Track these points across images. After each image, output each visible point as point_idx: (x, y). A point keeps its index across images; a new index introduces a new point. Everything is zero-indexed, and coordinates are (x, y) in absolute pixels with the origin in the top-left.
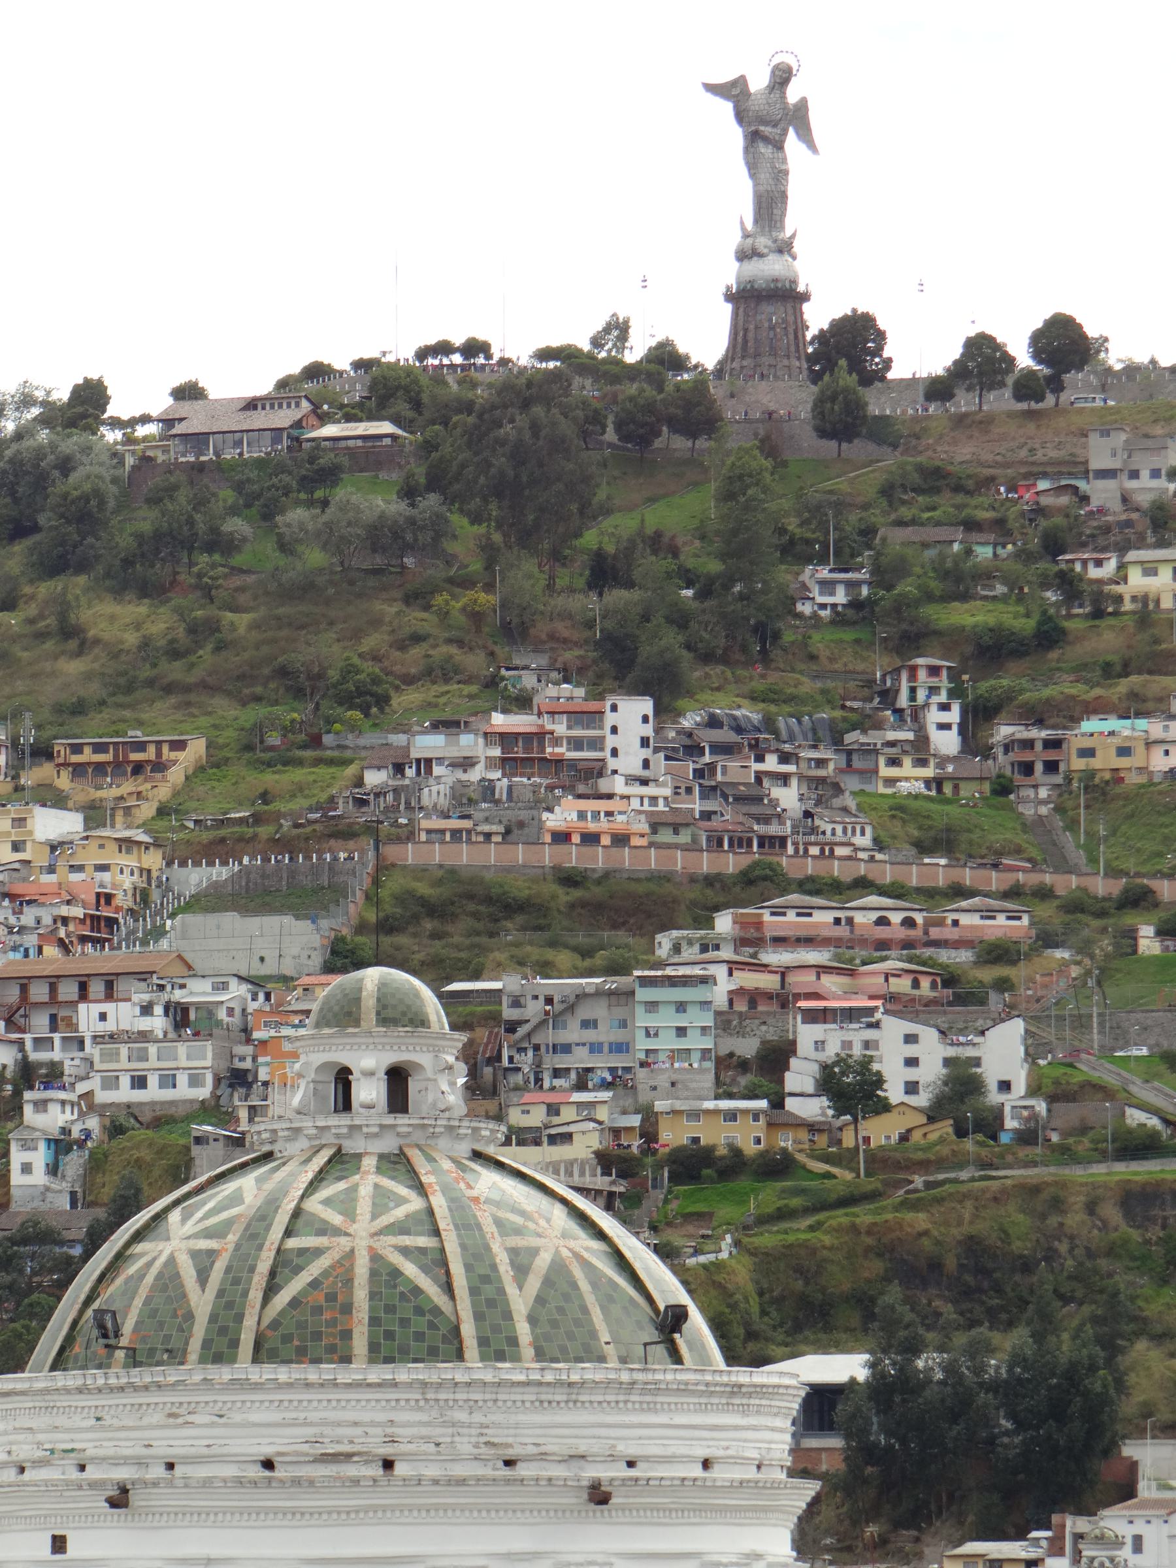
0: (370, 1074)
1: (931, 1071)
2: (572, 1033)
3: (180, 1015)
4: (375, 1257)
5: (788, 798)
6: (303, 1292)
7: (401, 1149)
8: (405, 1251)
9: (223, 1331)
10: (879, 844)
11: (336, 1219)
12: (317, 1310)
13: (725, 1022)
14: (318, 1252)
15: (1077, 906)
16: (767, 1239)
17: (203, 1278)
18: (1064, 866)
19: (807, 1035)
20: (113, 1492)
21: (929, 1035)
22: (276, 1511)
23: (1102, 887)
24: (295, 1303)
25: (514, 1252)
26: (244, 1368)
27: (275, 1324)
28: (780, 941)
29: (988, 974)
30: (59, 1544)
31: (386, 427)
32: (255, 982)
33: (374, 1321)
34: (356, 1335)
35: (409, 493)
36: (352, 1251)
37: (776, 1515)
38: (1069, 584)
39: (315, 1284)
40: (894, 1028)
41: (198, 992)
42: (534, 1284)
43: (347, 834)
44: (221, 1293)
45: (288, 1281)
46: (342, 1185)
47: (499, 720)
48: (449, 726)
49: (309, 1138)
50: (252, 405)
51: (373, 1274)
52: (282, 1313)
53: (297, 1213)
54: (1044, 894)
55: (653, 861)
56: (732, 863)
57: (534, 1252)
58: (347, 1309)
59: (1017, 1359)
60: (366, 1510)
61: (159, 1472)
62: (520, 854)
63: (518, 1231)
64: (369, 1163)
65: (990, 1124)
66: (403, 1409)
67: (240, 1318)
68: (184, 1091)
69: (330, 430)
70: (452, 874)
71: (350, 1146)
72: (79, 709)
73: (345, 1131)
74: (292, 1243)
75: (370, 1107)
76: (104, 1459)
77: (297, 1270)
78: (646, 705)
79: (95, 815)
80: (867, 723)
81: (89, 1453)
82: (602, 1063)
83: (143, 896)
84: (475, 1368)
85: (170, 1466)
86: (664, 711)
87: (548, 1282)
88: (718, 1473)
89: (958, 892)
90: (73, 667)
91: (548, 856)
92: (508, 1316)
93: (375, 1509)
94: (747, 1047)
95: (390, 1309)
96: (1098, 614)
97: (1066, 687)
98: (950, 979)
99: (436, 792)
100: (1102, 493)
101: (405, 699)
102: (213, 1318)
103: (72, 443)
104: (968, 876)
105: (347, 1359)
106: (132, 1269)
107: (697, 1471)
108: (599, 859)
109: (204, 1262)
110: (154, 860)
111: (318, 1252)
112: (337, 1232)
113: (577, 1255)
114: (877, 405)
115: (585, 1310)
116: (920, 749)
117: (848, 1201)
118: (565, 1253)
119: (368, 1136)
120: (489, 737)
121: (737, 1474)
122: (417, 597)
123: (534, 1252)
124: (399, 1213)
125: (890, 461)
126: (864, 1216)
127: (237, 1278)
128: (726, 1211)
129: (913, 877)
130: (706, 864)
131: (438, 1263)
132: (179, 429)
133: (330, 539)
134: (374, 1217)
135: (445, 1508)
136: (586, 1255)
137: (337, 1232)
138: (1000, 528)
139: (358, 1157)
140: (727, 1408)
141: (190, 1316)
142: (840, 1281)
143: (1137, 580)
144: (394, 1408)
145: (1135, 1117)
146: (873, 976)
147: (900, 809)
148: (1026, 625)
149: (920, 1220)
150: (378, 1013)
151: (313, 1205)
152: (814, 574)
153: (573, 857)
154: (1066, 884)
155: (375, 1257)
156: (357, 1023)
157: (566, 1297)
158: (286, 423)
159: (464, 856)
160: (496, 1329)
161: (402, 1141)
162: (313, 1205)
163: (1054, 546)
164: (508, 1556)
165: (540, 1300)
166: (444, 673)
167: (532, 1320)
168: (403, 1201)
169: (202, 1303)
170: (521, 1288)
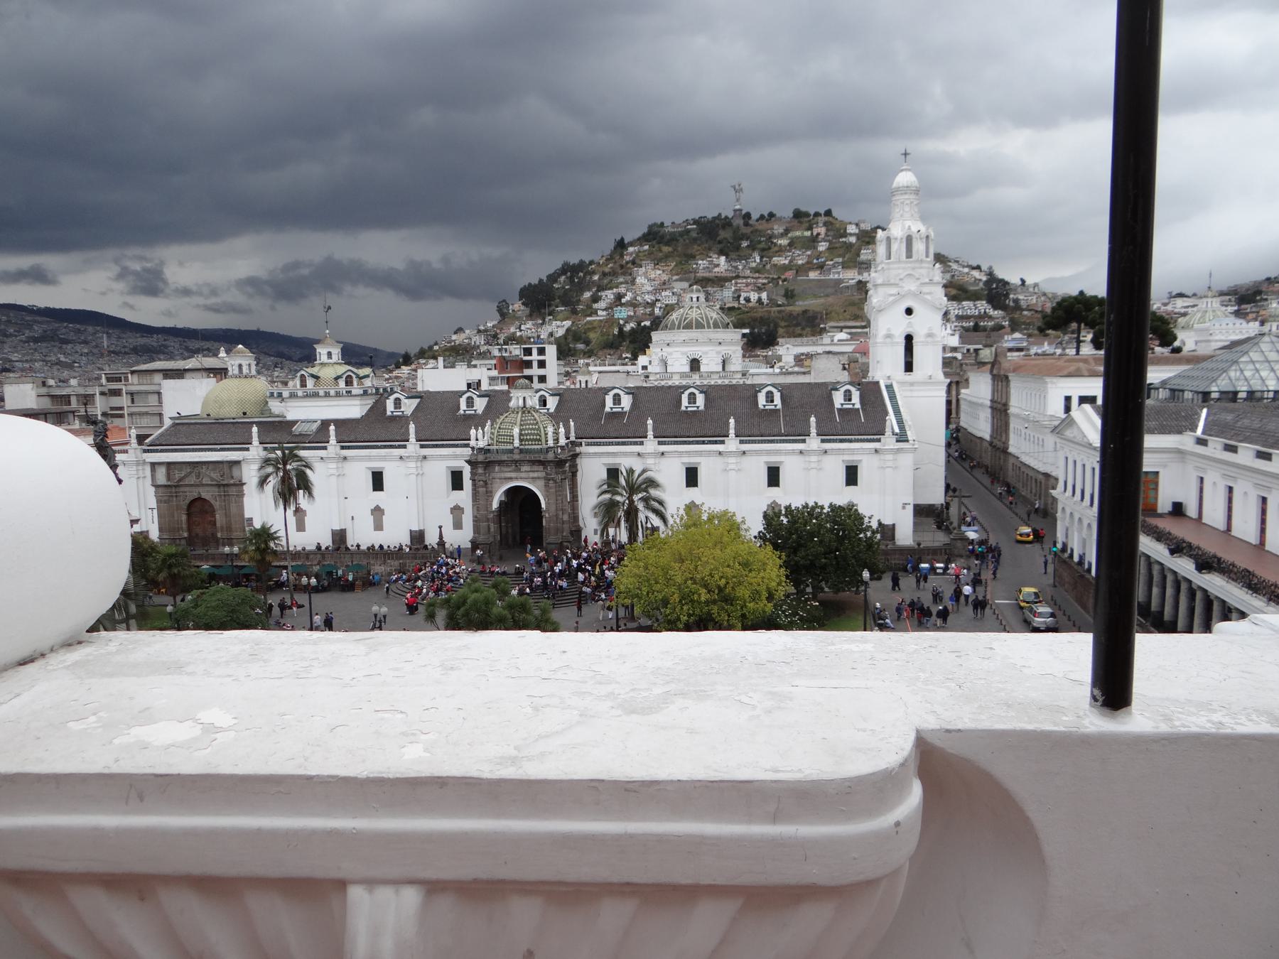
1: (756, 298)
2: (716, 294)
3: (673, 293)
5: (740, 267)
10: (751, 272)
13: (734, 293)
15: (773, 279)
16: (739, 317)
18: (771, 274)
19: (742, 294)
21: (756, 294)
23: (775, 277)
28: (740, 283)
29: (763, 286)
31: (695, 226)
32: (681, 289)
35: (698, 234)
38: (772, 243)
40: (752, 293)
41: (675, 290)
43: (691, 272)
47: (708, 259)
48: (703, 260)
54: (769, 278)
55: (726, 275)
56: (734, 275)
59: (766, 330)
62: (710, 274)
65: (763, 303)
68: (674, 302)
69: (689, 227)
70: (703, 277)
72: (662, 259)
78: (724, 257)
79: (663, 271)
80: (749, 259)
82: (720, 298)
83: (669, 280)
86: (727, 258)
89: (759, 278)
90: (661, 254)
91: (713, 275)
94: (736, 296)
96: (775, 246)
97: (771, 254)
98: (758, 287)
99: (701, 268)
100: (776, 232)
101: (697, 257)
103: (659, 229)
104: (760, 276)
108: (719, 275)
109: (677, 319)
110: (670, 276)
114: (751, 222)
116: (755, 261)
117: (747, 312)
120: (707, 261)
122: (699, 245)
125: (752, 229)
126: (749, 314)
127: (681, 320)
128: (733, 314)
129: (754, 276)
130: (731, 275)
131: (702, 318)
133: (688, 239)
138: (764, 236)
142: (747, 321)
143: (779, 242)
145: (779, 303)
146: (750, 287)
147: (753, 268)
148: (767, 247)
149: (755, 314)
152: (743, 242)
153: (716, 275)
154: (771, 276)
159: (705, 275)
163: (770, 238)
166: (702, 254)
169: (677, 323)
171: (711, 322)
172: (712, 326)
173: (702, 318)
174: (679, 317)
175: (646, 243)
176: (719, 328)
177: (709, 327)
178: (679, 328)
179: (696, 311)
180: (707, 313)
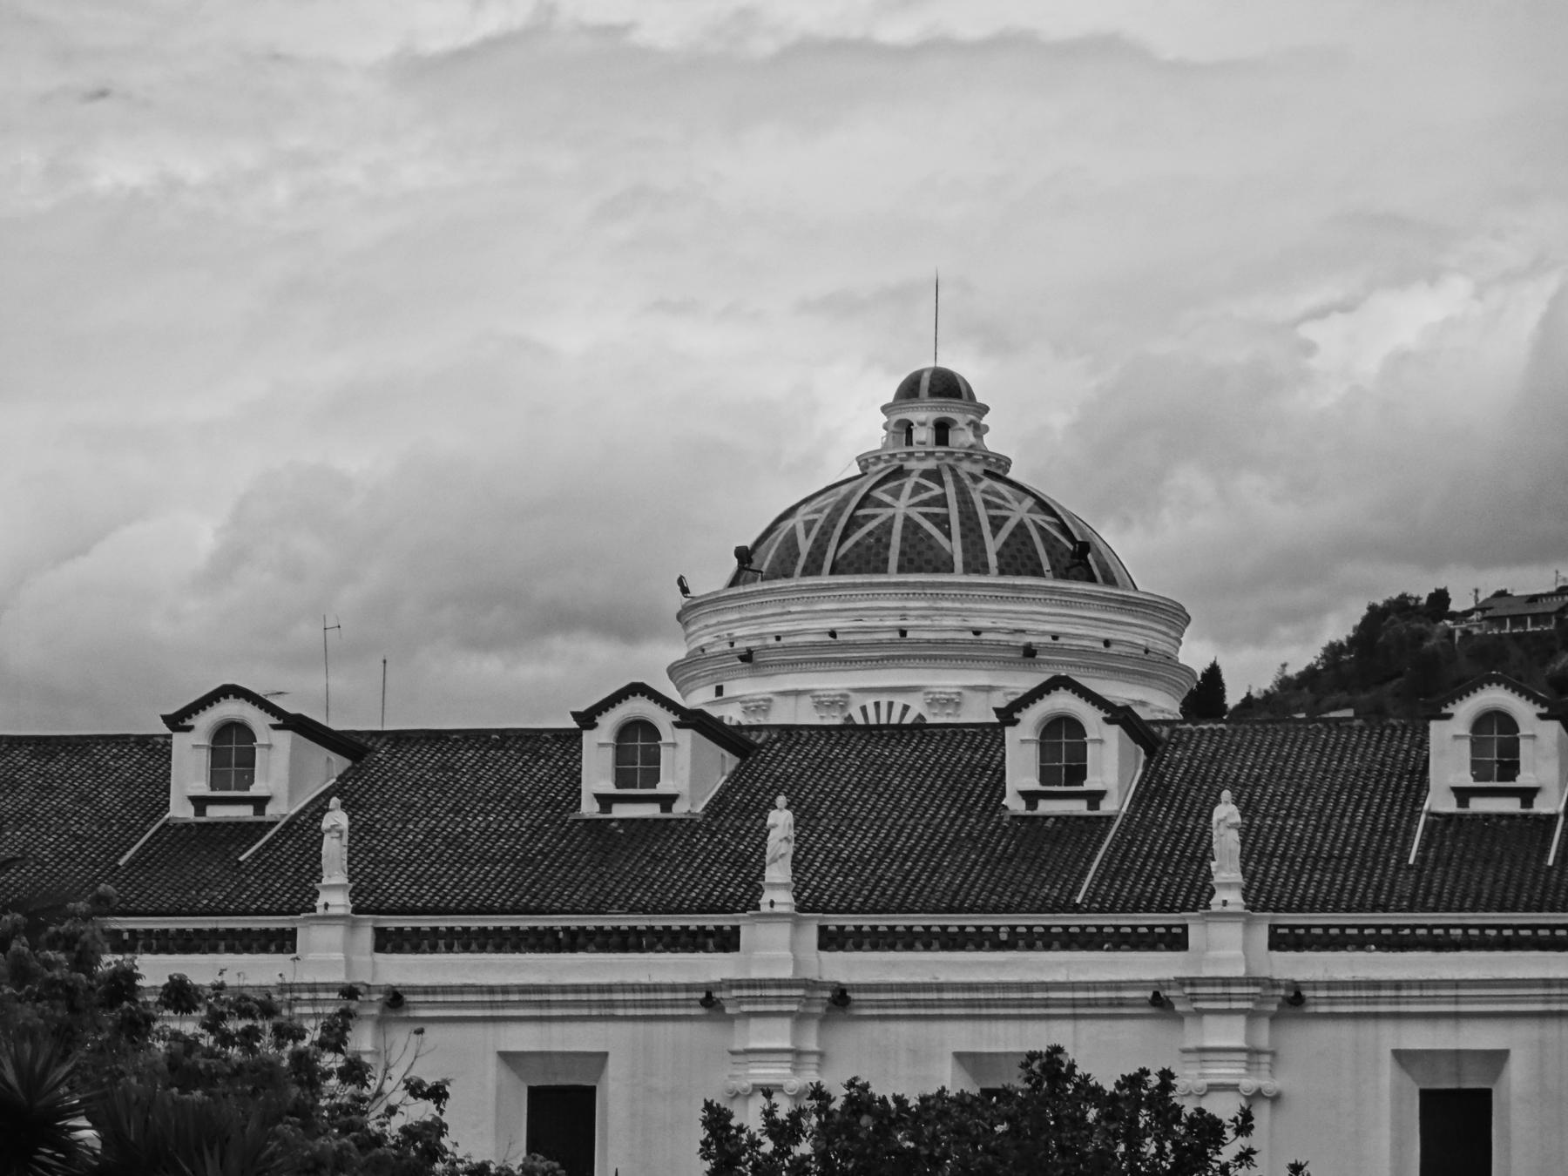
0: (922, 424)
4: (907, 519)
6: (864, 538)
7: (938, 466)
8: (925, 515)
9: (814, 561)
11: (887, 499)
12: (869, 548)
14: (874, 517)
17: (808, 533)
20: (744, 652)
22: (840, 660)
24: (857, 544)
25: (992, 519)
26: (825, 579)
27: (845, 556)
30: (719, 691)
33: (902, 553)
34: (890, 561)
36: (894, 516)
37: (1156, 681)
39: (870, 534)
42: (1004, 534)
44: (816, 540)
45: (854, 532)
46: (896, 483)
49: (886, 461)
50: (1533, 599)
51: (905, 527)
52: (850, 550)
57: (1006, 518)
58: (887, 546)
60: (888, 658)
61: (772, 641)
63: (999, 507)
64: (916, 474)
66: (911, 599)
67: (824, 553)
71: (908, 465)
73: (904, 456)
74: (861, 512)
75: (923, 443)
76: (742, 637)
77: (862, 526)
81: (736, 635)
84: (958, 577)
85: (778, 638)
87: (1013, 534)
88: (1113, 649)
92: (984, 551)
95: (913, 546)
102: (810, 554)
105: (884, 571)
106: (772, 536)
109: (809, 526)
111: (874, 517)
112: (888, 505)
115: (1035, 552)
118: (1027, 521)
119: (920, 459)
123: (1006, 518)
124: (925, 496)
127: (825, 533)
131: (942, 522)
132: (1488, 613)
134: (911, 497)
135: (935, 658)
136: (1047, 527)
137: (888, 505)
139: (912, 471)
140: (1120, 611)
141: (798, 554)
144: (906, 599)
150: (930, 390)
151: (878, 494)
155: (907, 519)
161: (939, 462)
162: (878, 494)
164: (974, 688)
165: (1006, 544)
167: (999, 554)
168: (931, 489)
169: (805, 546)
170: (994, 536)
171: (992, 546)
172: (992, 560)
173: (942, 522)
174: (821, 518)
175: (1344, 696)
176: (1037, 572)
177: (976, 564)
178: (813, 568)
179: (918, 489)
180: (977, 498)
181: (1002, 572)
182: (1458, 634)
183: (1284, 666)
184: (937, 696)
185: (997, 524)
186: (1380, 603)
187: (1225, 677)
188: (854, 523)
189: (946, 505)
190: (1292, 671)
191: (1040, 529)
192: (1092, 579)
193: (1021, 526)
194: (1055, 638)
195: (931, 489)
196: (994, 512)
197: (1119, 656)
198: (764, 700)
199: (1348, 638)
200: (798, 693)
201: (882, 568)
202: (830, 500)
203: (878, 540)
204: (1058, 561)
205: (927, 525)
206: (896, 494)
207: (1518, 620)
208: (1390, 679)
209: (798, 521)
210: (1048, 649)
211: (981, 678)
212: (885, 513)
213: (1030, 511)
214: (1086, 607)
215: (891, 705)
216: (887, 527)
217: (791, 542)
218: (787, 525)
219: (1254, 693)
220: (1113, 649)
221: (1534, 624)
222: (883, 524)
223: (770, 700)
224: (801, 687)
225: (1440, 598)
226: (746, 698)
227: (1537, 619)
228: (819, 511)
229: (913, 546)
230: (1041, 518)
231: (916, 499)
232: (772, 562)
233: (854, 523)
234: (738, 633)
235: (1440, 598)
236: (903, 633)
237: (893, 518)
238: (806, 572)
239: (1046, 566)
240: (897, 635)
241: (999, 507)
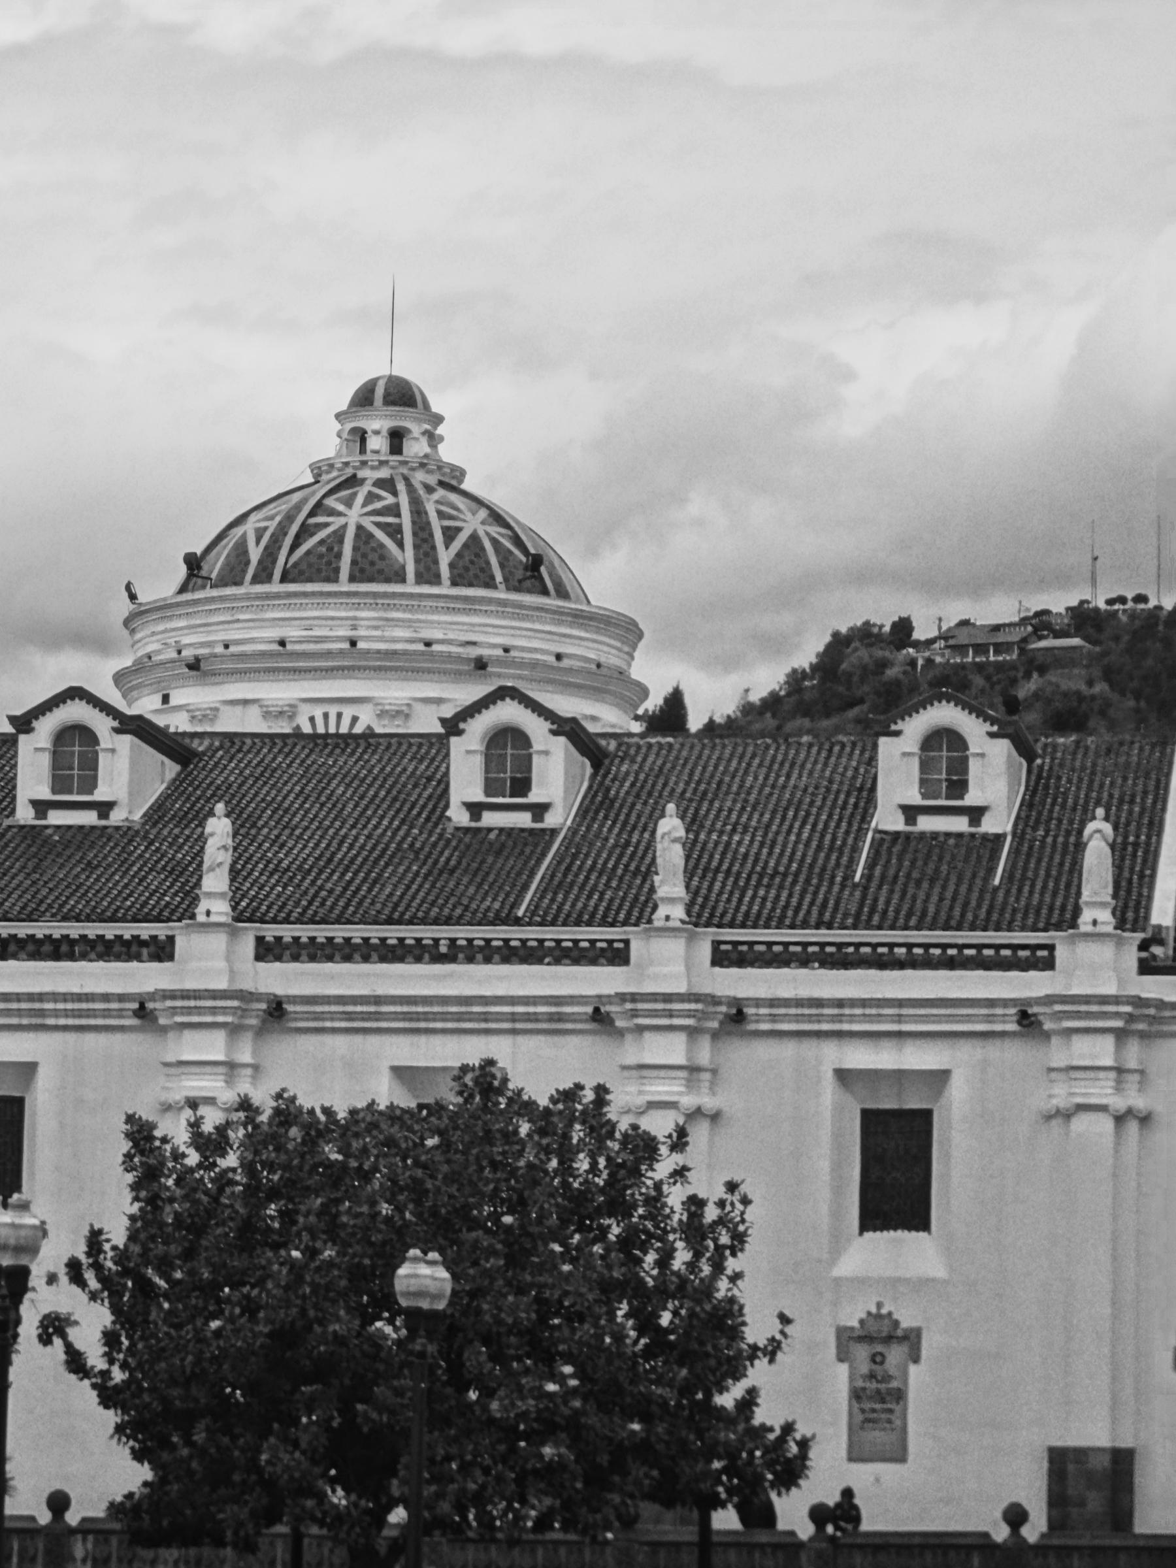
0: (377, 433)
4: (360, 528)
8: (378, 525)
9: (264, 569)
11: (341, 508)
12: (321, 556)
14: (327, 525)
17: (258, 542)
20: (192, 660)
24: (308, 553)
26: (275, 587)
27: (295, 565)
30: (166, 699)
31: (1076, 641)
33: (354, 562)
39: (322, 542)
42: (457, 545)
44: (266, 548)
49: (340, 470)
50: (997, 628)
51: (357, 536)
52: (301, 559)
53: (319, 505)
57: (459, 530)
58: (339, 556)
61: (219, 649)
63: (451, 518)
64: (369, 482)
69: (1043, 644)
71: (361, 474)
74: (312, 521)
75: (377, 452)
76: (190, 645)
77: (312, 535)
84: (411, 588)
85: (226, 646)
87: (466, 546)
88: (566, 663)
93: (343, 668)
95: (364, 556)
102: (260, 562)
107: (552, 659)
111: (327, 525)
112: (340, 514)
113: (488, 534)
115: (488, 563)
118: (481, 533)
119: (373, 468)
121: (577, 664)
124: (378, 505)
131: (395, 532)
132: (951, 642)
137: (340, 514)
140: (571, 625)
141: (248, 562)
150: (384, 397)
151: (331, 502)
155: (360, 528)
156: (371, 404)
157: (477, 555)
158: (1016, 639)
160: (428, 569)
162: (331, 502)
165: (459, 555)
167: (452, 566)
168: (385, 499)
170: (447, 548)
171: (445, 557)
173: (395, 532)
174: (273, 525)
176: (490, 584)
177: (427, 574)
178: (263, 575)
179: (371, 497)
180: (431, 509)
181: (454, 583)
182: (920, 662)
183: (747, 691)
184: (387, 707)
185: (450, 534)
186: (844, 630)
187: (688, 701)
188: (305, 531)
189: (398, 515)
190: (755, 697)
191: (495, 542)
192: (545, 592)
193: (474, 538)
194: (506, 650)
195: (385, 499)
196: (447, 523)
197: (570, 670)
198: (211, 709)
199: (811, 664)
200: (246, 702)
201: (333, 577)
202: (284, 506)
203: (330, 549)
204: (511, 573)
205: (380, 535)
206: (349, 503)
207: (980, 649)
208: (851, 705)
209: (249, 527)
210: (499, 662)
211: (430, 690)
212: (337, 522)
213: (483, 523)
214: (539, 620)
215: (339, 716)
216: (339, 536)
217: (241, 550)
218: (238, 532)
219: (718, 719)
220: (566, 663)
221: (996, 652)
222: (335, 532)
223: (217, 709)
224: (249, 696)
225: (903, 627)
226: (191, 707)
227: (999, 648)
228: (272, 518)
229: (364, 556)
230: (495, 530)
231: (369, 508)
232: (222, 569)
233: (305, 531)
234: (186, 640)
235: (903, 627)
236: (353, 643)
237: (345, 526)
238: (256, 580)
239: (499, 578)
240: (346, 645)
241: (451, 518)
